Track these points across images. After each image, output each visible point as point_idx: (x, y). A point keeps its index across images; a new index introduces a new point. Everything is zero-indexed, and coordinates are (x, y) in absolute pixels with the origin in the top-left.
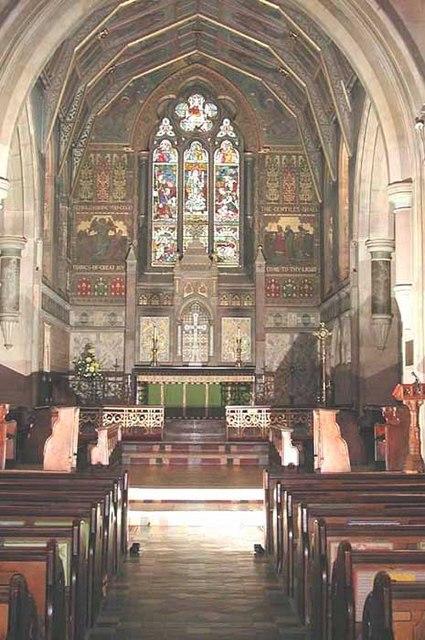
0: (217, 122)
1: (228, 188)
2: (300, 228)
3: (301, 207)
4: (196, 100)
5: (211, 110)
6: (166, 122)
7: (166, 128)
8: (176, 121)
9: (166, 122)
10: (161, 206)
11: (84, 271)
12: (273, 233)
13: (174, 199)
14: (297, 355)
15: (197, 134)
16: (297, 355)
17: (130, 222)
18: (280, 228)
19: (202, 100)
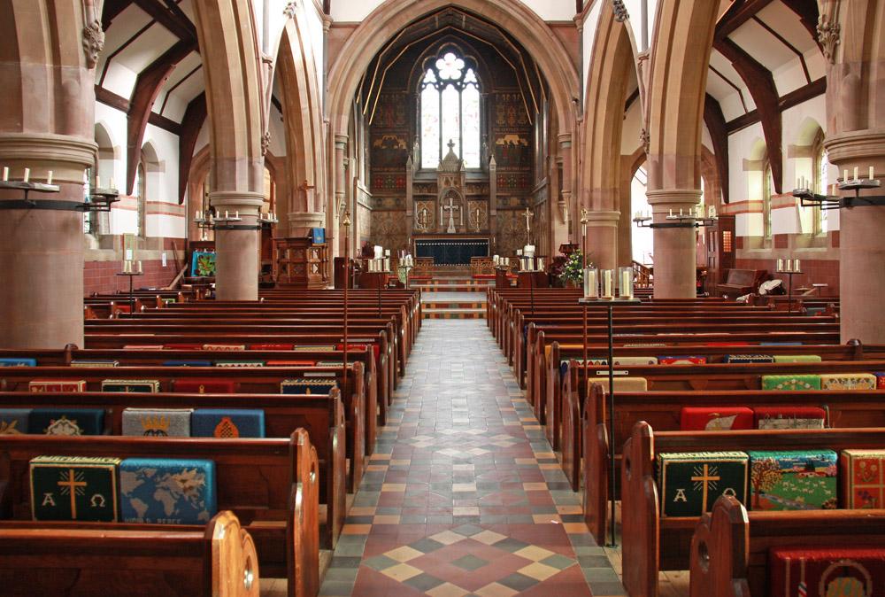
0: (464, 72)
2: (519, 142)
4: (450, 57)
5: (461, 63)
6: (430, 71)
7: (429, 76)
8: (436, 72)
9: (430, 71)
18: (506, 142)
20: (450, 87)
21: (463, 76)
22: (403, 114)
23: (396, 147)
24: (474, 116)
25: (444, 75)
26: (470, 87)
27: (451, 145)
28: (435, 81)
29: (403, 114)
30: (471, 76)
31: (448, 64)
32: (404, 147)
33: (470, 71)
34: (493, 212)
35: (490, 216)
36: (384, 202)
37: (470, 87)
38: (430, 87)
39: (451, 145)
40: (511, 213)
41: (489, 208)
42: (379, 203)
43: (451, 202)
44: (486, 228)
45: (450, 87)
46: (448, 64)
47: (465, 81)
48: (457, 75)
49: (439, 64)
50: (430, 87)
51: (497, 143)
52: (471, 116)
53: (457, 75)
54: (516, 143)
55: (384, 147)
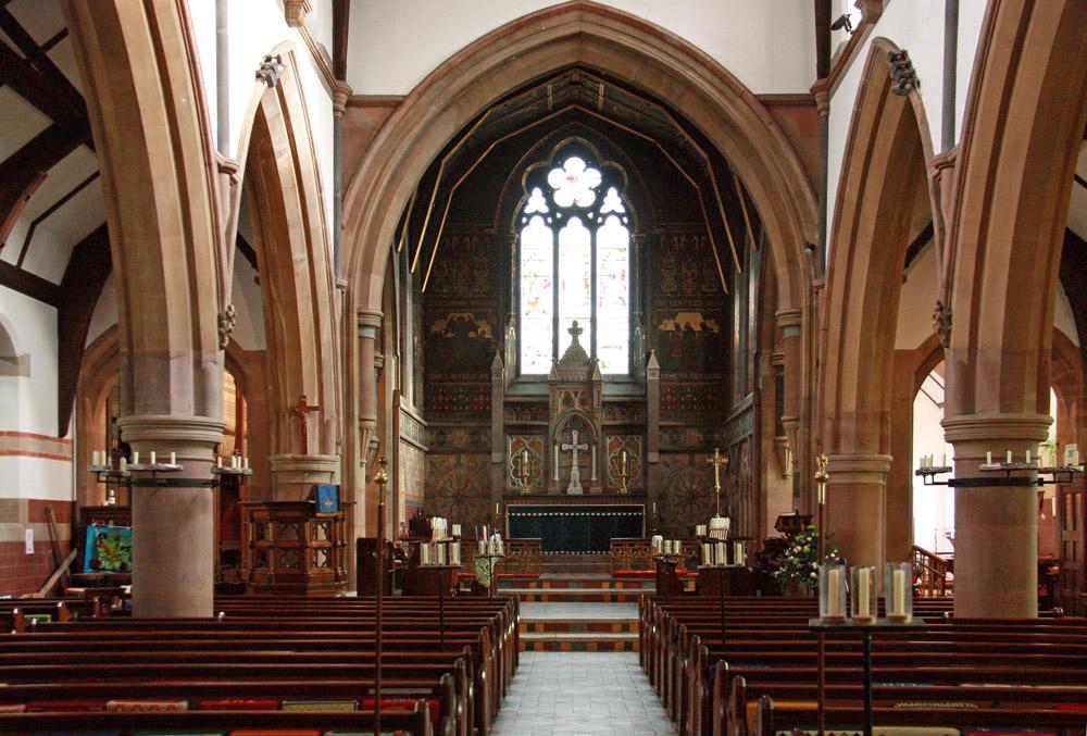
4: (575, 164)
5: (594, 177)
6: (537, 192)
7: (536, 201)
8: (548, 193)
9: (537, 192)
10: (533, 300)
20: (575, 223)
21: (599, 202)
25: (562, 200)
27: (575, 331)
28: (545, 210)
31: (570, 179)
33: (612, 192)
34: (653, 457)
35: (646, 463)
38: (537, 222)
39: (575, 331)
40: (685, 458)
43: (575, 437)
44: (640, 485)
46: (570, 179)
48: (587, 200)
50: (537, 222)
53: (587, 200)
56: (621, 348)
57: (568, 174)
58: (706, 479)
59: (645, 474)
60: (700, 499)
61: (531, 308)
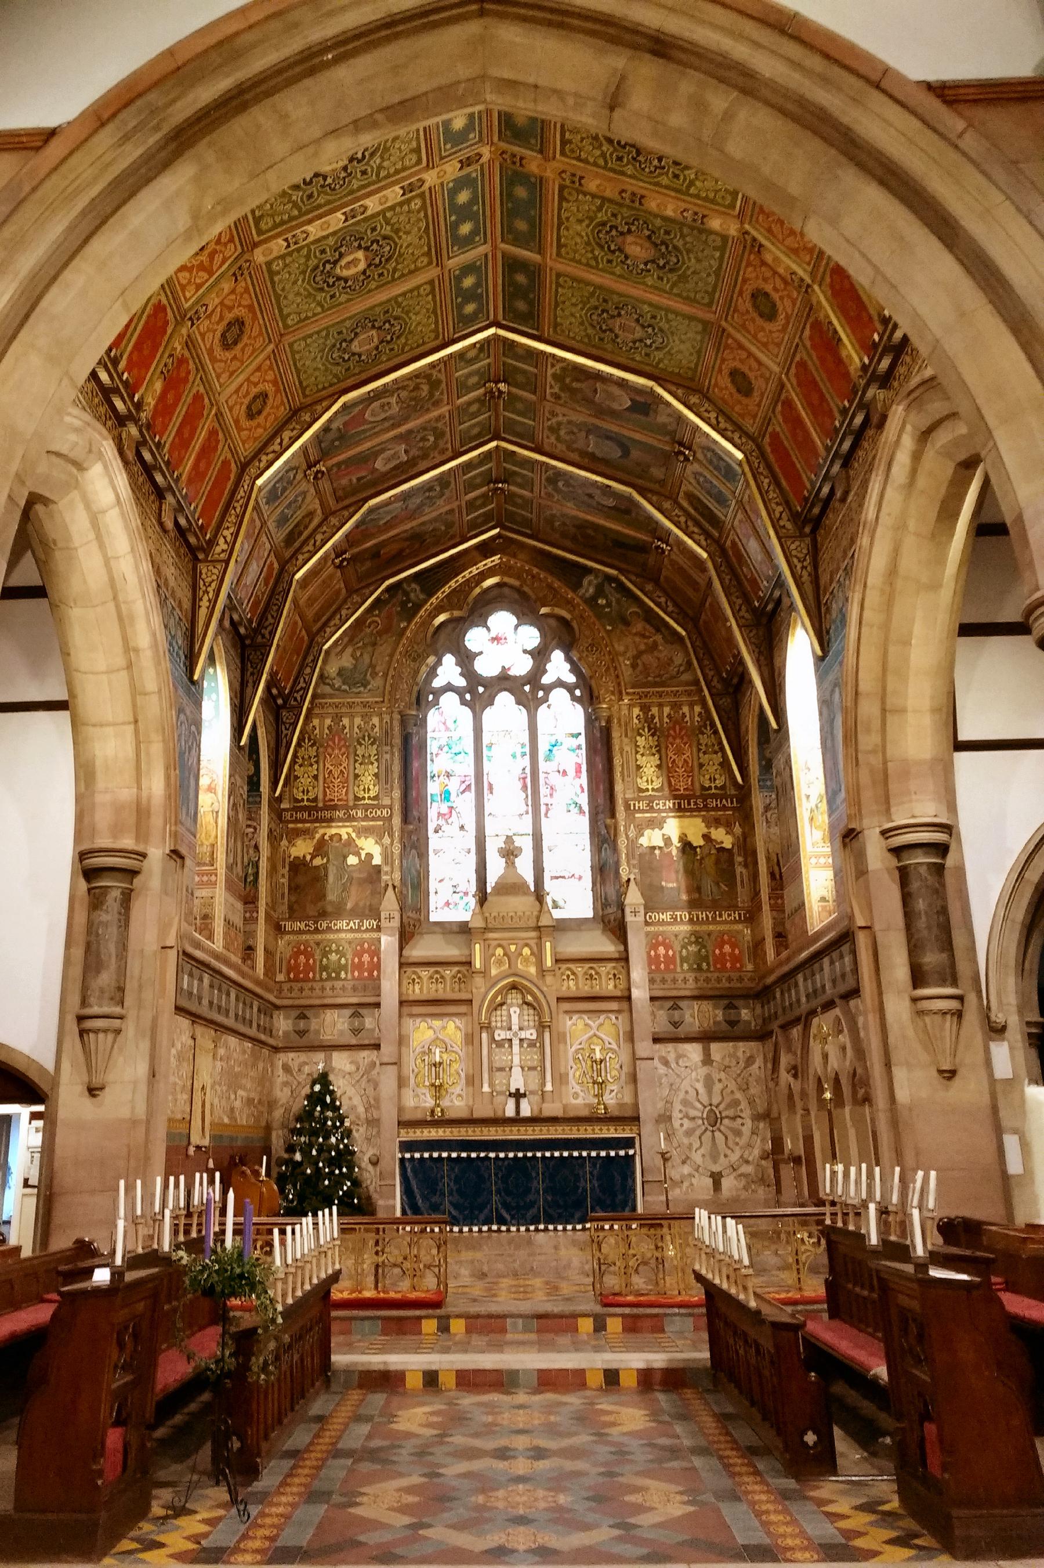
0: (540, 655)
1: (565, 773)
2: (706, 837)
3: (705, 800)
4: (502, 620)
5: (531, 636)
6: (449, 660)
7: (449, 671)
8: (466, 659)
9: (449, 660)
11: (300, 932)
12: (654, 848)
13: (467, 793)
14: (718, 1087)
15: (504, 681)
16: (718, 1087)
17: (387, 840)
18: (668, 841)
19: (514, 620)
20: (505, 699)
22: (373, 769)
23: (352, 860)
24: (572, 772)
25: (486, 667)
26: (559, 696)
27: (510, 853)
29: (373, 769)
30: (558, 666)
32: (377, 860)
34: (644, 1047)
35: (635, 1058)
36: (314, 1024)
37: (559, 696)
38: (449, 700)
39: (510, 853)
40: (693, 1052)
41: (630, 1037)
42: (302, 1024)
44: (628, 1099)
45: (505, 699)
46: (496, 639)
47: (546, 680)
49: (475, 638)
50: (449, 700)
51: (644, 841)
52: (565, 773)
54: (698, 841)
55: (318, 861)
56: (580, 878)
57: (493, 634)
58: (732, 1086)
59: (633, 1078)
60: (726, 1121)
61: (441, 822)
